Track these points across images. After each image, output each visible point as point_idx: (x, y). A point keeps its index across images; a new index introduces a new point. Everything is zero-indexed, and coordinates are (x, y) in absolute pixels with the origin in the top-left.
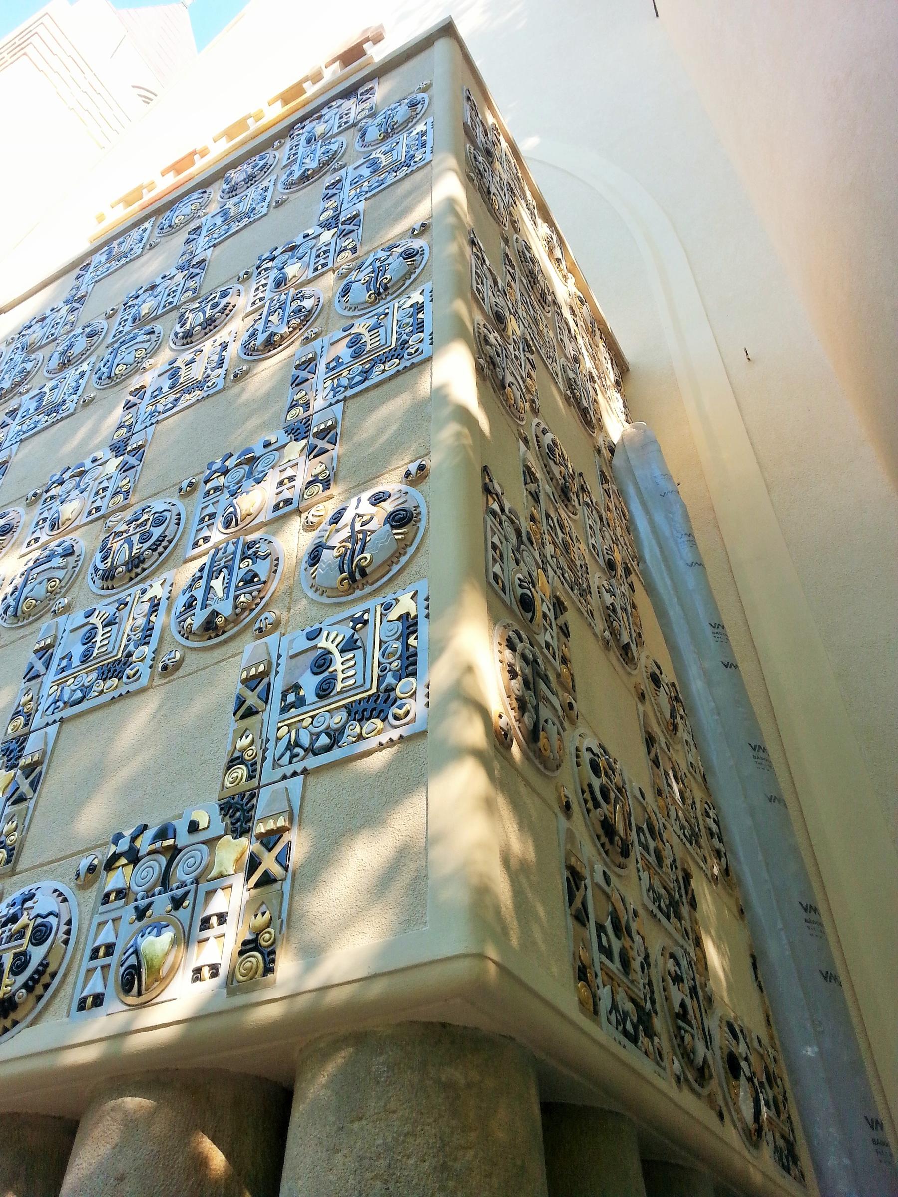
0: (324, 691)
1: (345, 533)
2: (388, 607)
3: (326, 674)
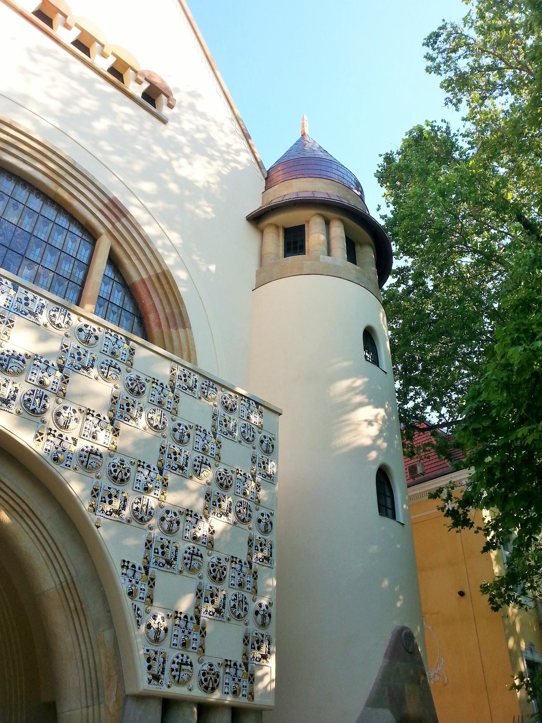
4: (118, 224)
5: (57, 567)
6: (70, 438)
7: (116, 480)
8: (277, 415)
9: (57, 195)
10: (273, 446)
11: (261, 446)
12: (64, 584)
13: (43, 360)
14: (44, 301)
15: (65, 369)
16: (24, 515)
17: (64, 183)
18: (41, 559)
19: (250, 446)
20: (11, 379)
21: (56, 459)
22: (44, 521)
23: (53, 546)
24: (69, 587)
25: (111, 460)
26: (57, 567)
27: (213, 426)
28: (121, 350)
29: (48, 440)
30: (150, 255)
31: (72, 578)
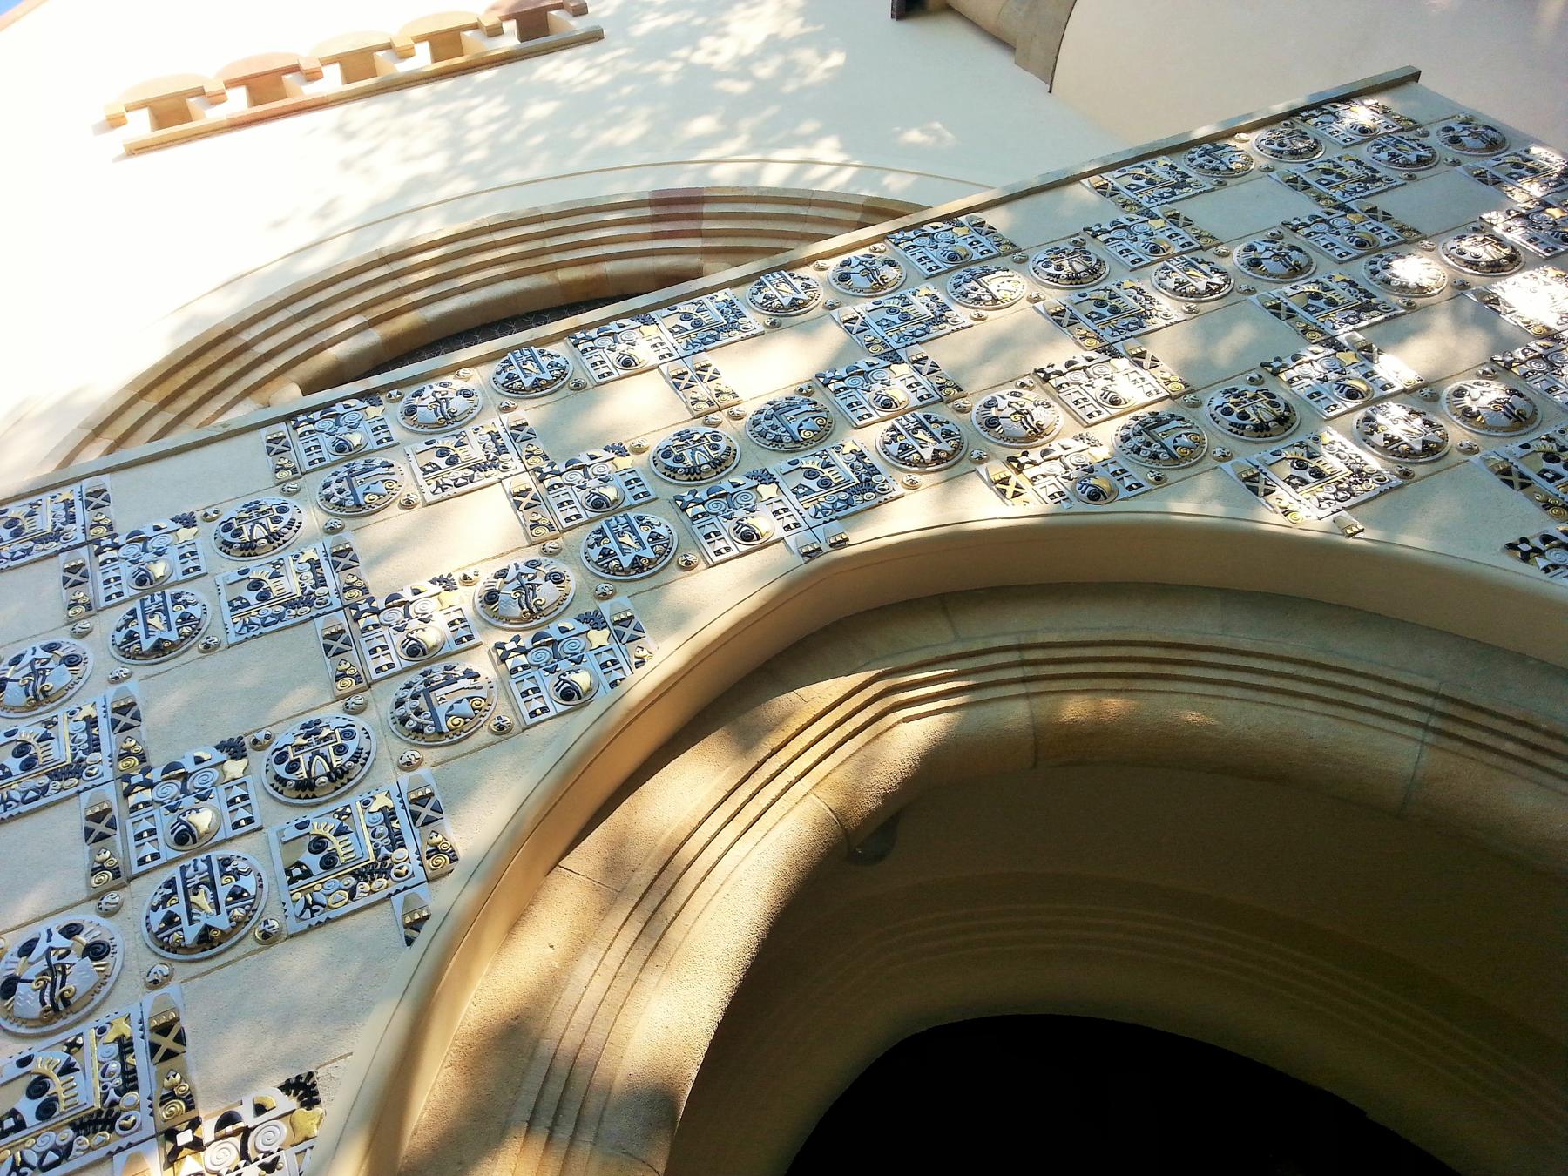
0: (46, 1112)
1: (42, 965)
2: (102, 1031)
3: (45, 1097)
4: (706, 225)
5: (1374, 704)
6: (1069, 442)
7: (1268, 429)
8: (1413, 84)
9: (566, 287)
10: (1487, 127)
11: (1464, 147)
12: (1435, 722)
13: (842, 372)
14: (721, 296)
15: (901, 353)
16: (1167, 669)
17: (555, 258)
18: (1316, 718)
19: (1442, 167)
20: (827, 446)
21: (1096, 495)
22: (1225, 641)
23: (1304, 671)
24: (1452, 718)
25: (1205, 410)
26: (1374, 704)
27: (1318, 199)
28: (960, 243)
29: (1033, 480)
30: (812, 212)
31: (1435, 695)
